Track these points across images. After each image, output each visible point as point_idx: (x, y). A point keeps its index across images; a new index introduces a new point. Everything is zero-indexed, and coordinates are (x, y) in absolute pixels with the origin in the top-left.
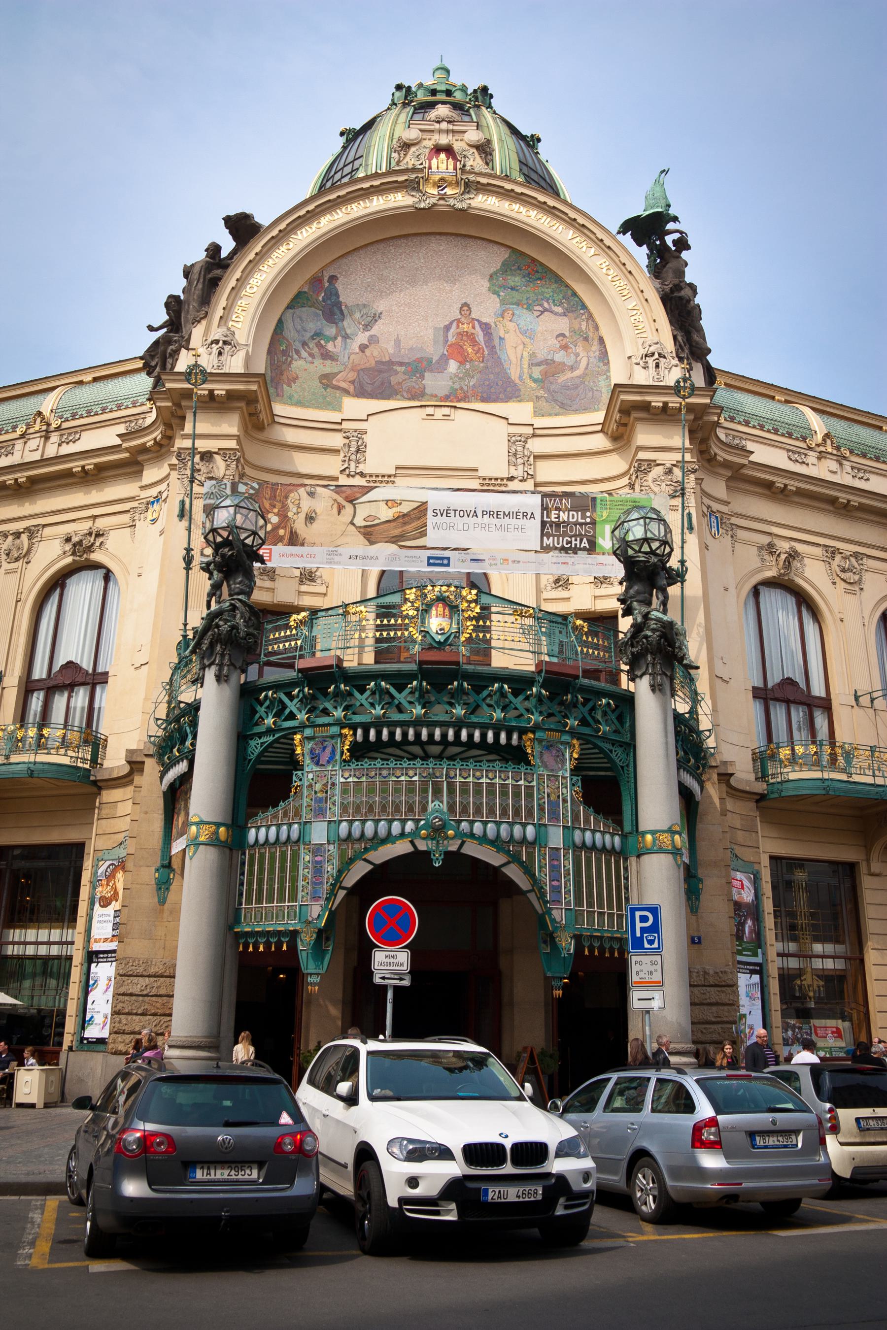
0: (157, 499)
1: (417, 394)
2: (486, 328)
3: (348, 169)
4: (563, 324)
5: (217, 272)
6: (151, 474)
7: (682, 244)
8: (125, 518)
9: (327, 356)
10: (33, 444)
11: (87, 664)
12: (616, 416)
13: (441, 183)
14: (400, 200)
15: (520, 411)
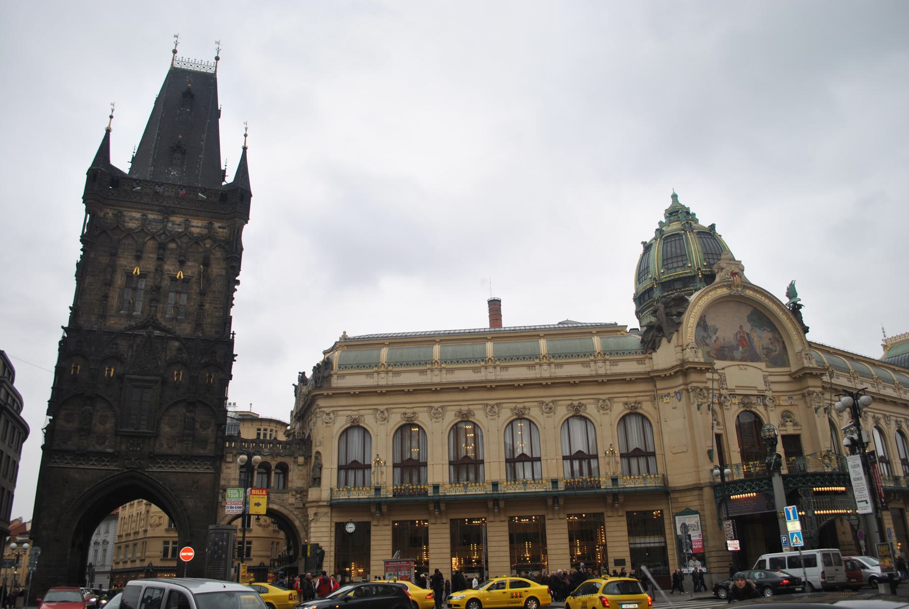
0: (668, 395)
1: (733, 359)
2: (748, 334)
3: (680, 259)
4: (770, 335)
5: (668, 310)
6: (659, 385)
7: (800, 306)
8: (648, 398)
9: (707, 345)
10: (600, 364)
11: (643, 449)
12: (801, 374)
13: (737, 286)
14: (724, 291)
15: (762, 365)
